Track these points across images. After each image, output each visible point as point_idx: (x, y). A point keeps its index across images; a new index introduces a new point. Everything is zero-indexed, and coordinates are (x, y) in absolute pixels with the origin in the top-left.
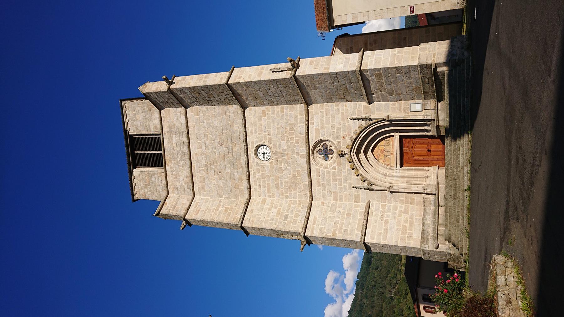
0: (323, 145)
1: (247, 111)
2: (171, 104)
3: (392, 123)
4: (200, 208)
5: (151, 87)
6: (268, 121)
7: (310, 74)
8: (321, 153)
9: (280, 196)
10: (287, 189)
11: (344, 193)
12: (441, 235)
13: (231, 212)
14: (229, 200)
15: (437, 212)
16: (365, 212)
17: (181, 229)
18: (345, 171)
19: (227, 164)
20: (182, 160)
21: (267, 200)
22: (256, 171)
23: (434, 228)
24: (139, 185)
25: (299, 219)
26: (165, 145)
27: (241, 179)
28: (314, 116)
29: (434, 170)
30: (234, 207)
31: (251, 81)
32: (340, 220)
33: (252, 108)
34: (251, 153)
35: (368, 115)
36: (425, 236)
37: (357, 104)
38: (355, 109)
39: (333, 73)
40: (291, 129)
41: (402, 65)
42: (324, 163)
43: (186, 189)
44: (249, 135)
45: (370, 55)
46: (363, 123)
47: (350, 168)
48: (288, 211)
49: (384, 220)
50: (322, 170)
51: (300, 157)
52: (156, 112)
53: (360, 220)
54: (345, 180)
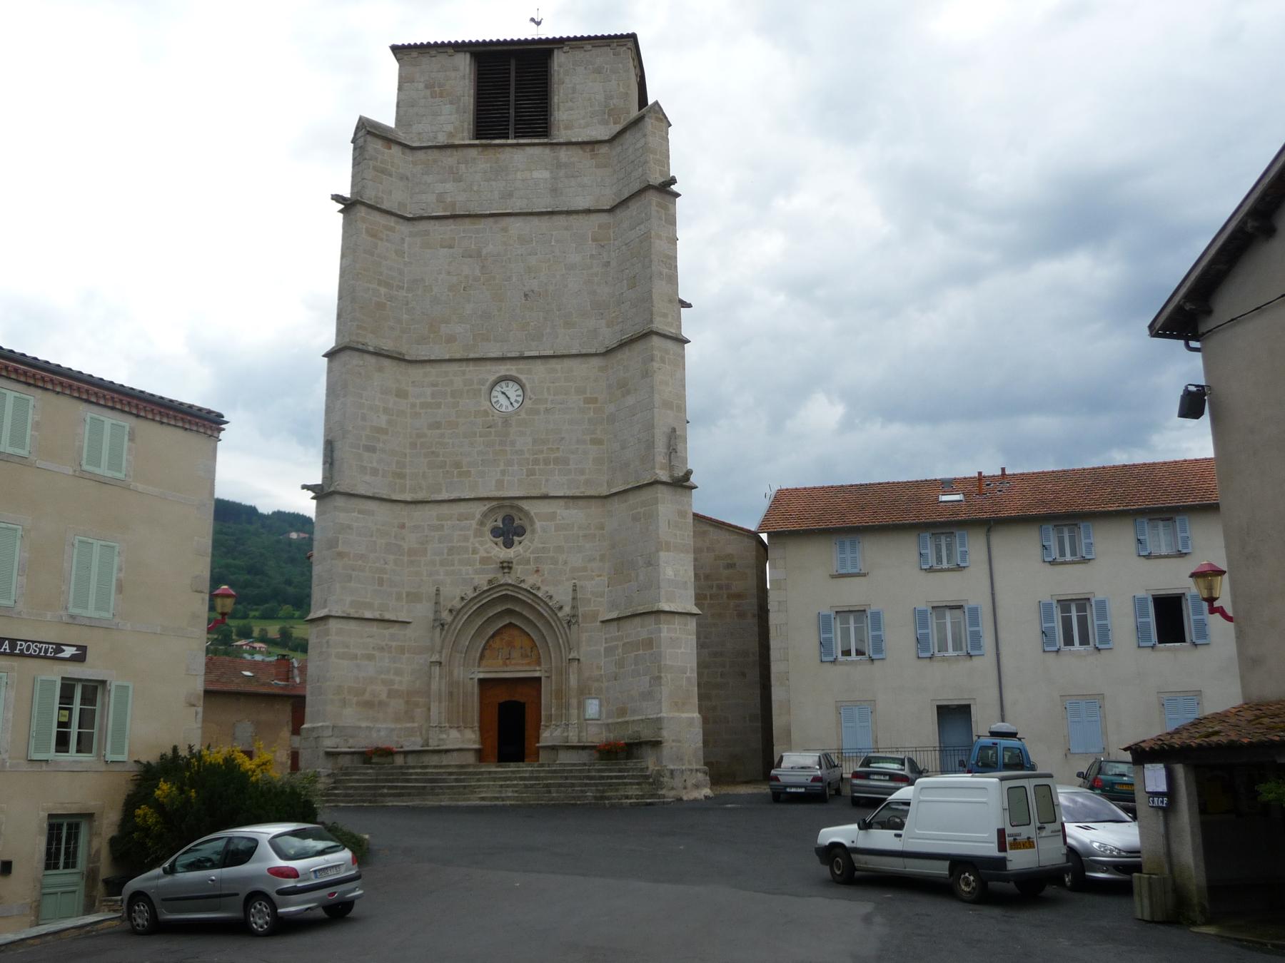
4: (382, 240)
40: (556, 461)
42: (486, 529)
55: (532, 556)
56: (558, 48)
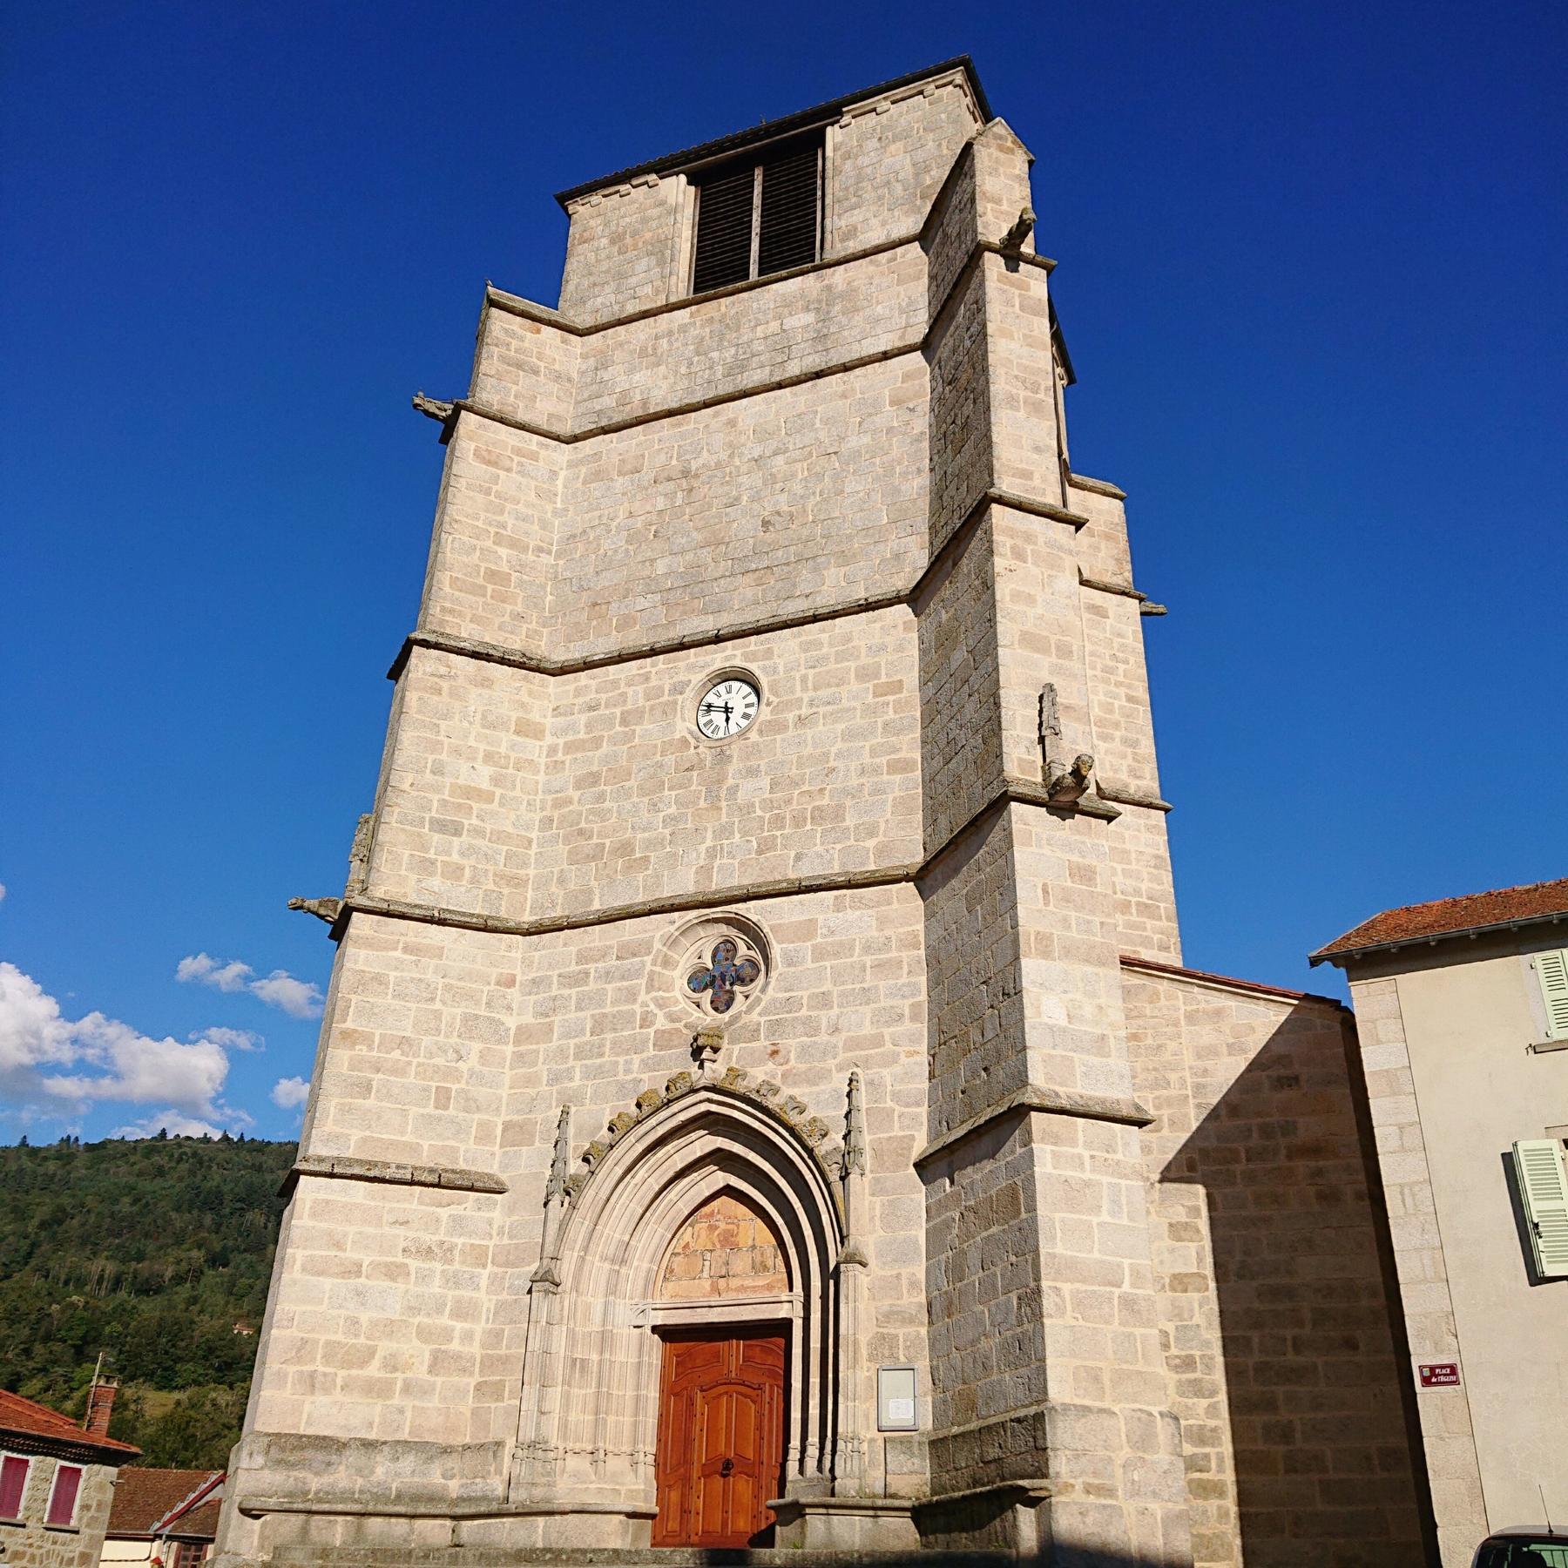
1: (904, 609)
2: (940, 278)
4: (509, 470)
5: (1001, 170)
6: (855, 709)
7: (1017, 866)
9: (549, 797)
10: (578, 823)
11: (542, 1070)
14: (543, 587)
17: (417, 401)
19: (689, 557)
20: (711, 368)
21: (538, 743)
22: (654, 682)
24: (623, 210)
26: (774, 286)
27: (626, 623)
28: (870, 912)
31: (998, 605)
33: (915, 635)
34: (729, 652)
39: (1020, 977)
41: (1046, 1321)
42: (677, 973)
44: (800, 635)
45: (1119, 1156)
47: (644, 1088)
50: (643, 964)
51: (702, 863)
52: (912, 223)
54: (599, 1072)
55: (762, 1020)
56: (832, 124)
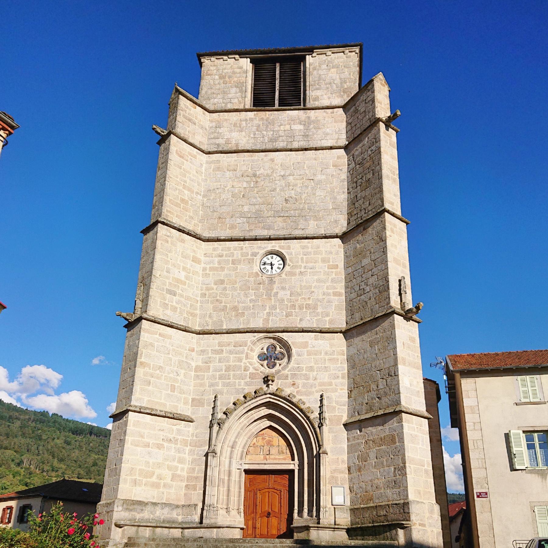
0: (282, 353)
1: (338, 241)
2: (353, 125)
3: (315, 459)
4: (187, 160)
6: (321, 272)
8: (270, 349)
9: (204, 286)
10: (216, 297)
11: (207, 382)
12: (137, 532)
13: (180, 208)
14: (199, 207)
15: (173, 526)
16: (177, 414)
18: (242, 384)
19: (257, 207)
20: (263, 137)
21: (199, 266)
22: (244, 251)
23: (148, 521)
24: (224, 66)
25: (169, 312)
26: (288, 112)
27: (232, 227)
28: (327, 342)
29: (239, 522)
30: (188, 214)
32: (166, 374)
33: (343, 250)
34: (273, 244)
35: (327, 421)
36: (136, 506)
37: (344, 406)
38: (337, 402)
43: (217, 141)
44: (300, 243)
46: (316, 414)
47: (246, 391)
48: (182, 296)
49: (164, 443)
50: (244, 350)
51: (265, 317)
52: (341, 101)
53: (165, 405)
54: (228, 385)
55: (289, 373)
56: (309, 55)
